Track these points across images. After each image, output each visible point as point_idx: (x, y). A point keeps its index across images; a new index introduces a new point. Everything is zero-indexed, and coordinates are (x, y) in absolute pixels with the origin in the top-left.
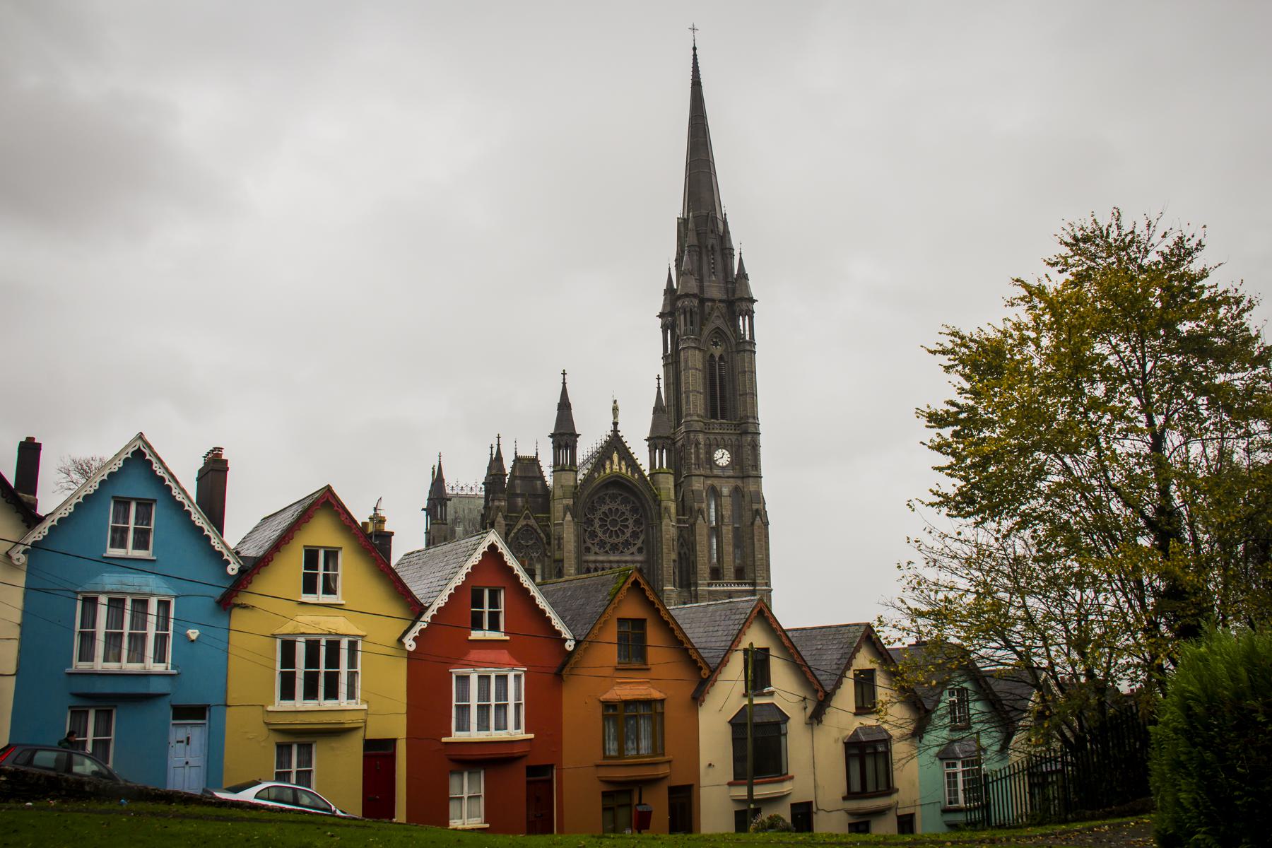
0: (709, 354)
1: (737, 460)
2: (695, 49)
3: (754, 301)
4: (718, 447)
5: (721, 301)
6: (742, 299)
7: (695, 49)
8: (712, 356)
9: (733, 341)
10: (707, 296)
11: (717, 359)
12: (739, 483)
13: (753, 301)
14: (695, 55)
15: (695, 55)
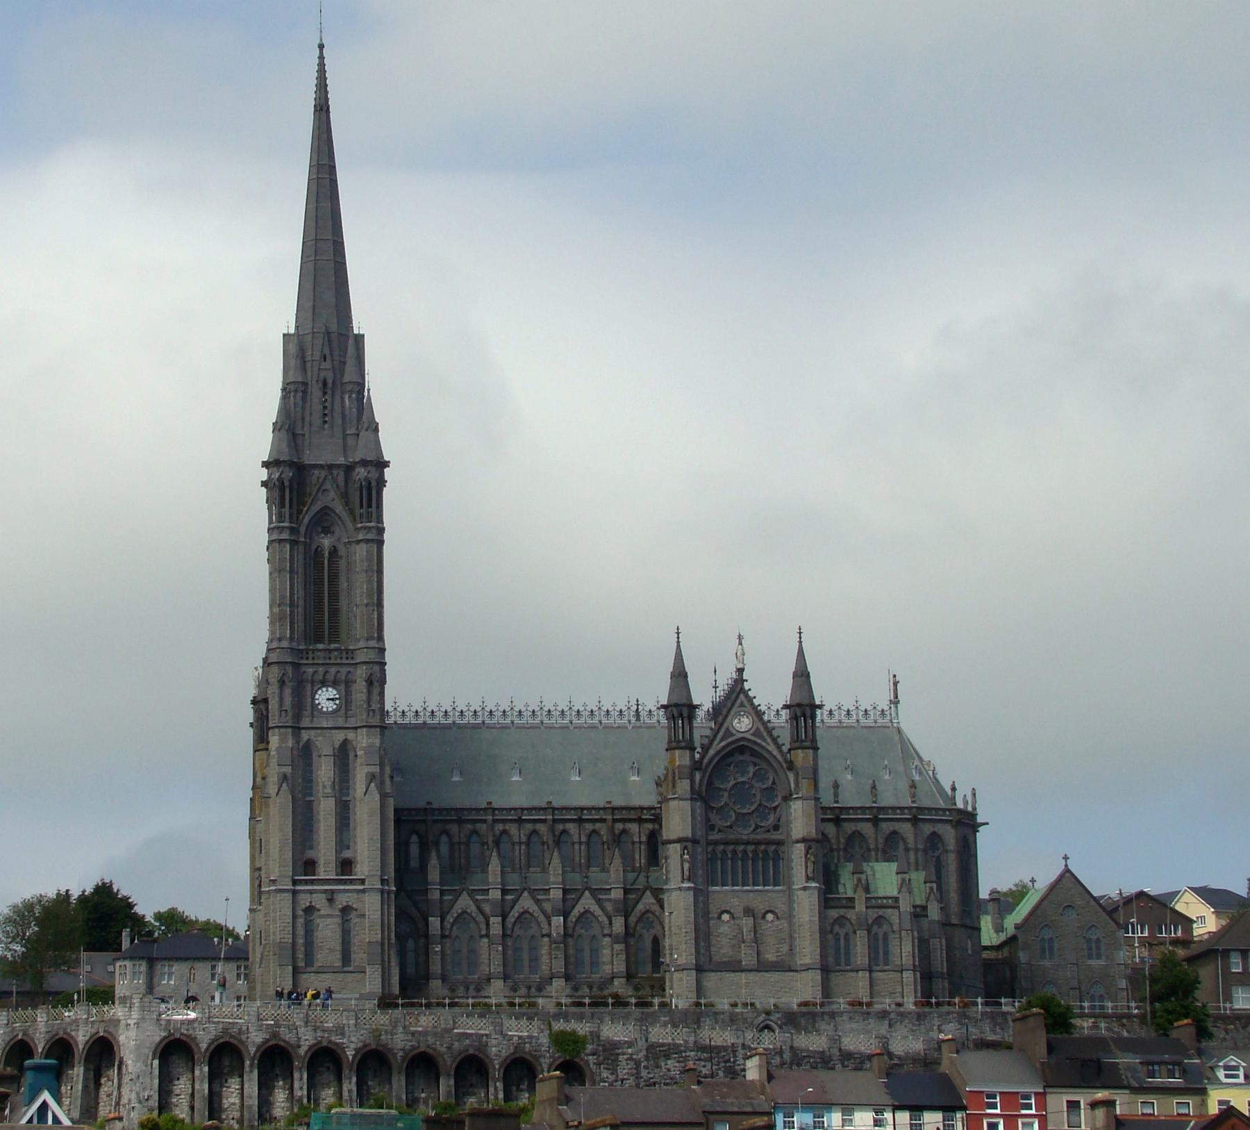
0: (314, 547)
1: (346, 702)
2: (321, 47)
3: (386, 464)
4: (324, 683)
5: (331, 467)
6: (364, 463)
7: (321, 47)
8: (318, 552)
9: (350, 525)
10: (308, 459)
11: (327, 554)
12: (351, 735)
13: (386, 464)
14: (321, 58)
15: (321, 58)
